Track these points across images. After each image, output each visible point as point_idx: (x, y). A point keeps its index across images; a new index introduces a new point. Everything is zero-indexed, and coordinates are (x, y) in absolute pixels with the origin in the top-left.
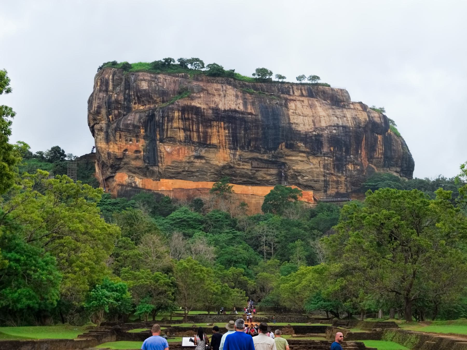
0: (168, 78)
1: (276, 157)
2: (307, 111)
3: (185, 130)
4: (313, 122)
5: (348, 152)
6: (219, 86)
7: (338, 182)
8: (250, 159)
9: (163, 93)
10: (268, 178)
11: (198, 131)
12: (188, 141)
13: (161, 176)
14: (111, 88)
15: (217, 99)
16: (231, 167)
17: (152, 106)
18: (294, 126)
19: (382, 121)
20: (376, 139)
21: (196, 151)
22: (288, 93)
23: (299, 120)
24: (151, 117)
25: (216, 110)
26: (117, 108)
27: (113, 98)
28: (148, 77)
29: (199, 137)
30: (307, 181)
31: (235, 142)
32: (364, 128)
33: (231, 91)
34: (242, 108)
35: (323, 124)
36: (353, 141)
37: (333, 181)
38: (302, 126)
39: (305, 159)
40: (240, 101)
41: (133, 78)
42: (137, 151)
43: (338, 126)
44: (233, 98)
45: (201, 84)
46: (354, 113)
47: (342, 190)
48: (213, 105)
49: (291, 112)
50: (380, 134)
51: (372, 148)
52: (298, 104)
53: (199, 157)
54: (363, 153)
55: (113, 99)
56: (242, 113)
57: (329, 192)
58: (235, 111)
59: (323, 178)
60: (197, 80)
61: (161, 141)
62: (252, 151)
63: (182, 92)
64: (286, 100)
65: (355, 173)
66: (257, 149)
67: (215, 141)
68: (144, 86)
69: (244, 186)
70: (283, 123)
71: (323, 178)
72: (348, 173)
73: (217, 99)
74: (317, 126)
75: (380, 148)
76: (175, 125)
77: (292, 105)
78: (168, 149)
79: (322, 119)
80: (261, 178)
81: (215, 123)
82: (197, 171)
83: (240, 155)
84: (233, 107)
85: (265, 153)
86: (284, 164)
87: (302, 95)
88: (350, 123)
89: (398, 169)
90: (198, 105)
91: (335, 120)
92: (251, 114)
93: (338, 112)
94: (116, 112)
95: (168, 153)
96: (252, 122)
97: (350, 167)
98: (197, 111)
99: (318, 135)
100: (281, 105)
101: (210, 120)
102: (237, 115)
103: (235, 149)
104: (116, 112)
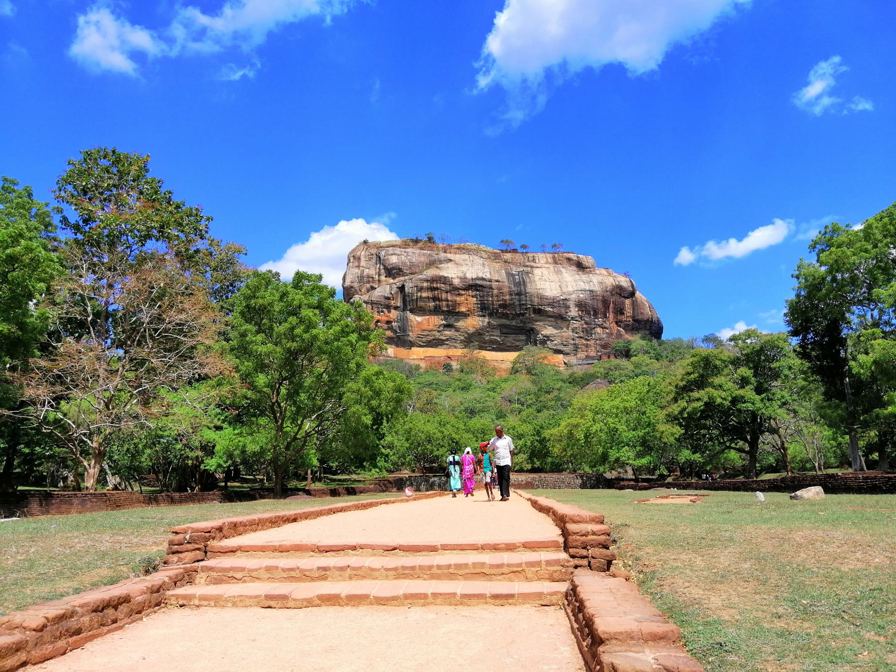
0: (418, 251)
1: (525, 323)
2: (554, 277)
3: (435, 299)
4: (560, 287)
5: (596, 314)
6: (466, 257)
7: (587, 346)
8: (499, 325)
9: (412, 265)
10: (517, 343)
11: (447, 300)
12: (436, 311)
13: (411, 345)
14: (363, 263)
15: (464, 268)
16: (480, 334)
17: (402, 278)
18: (541, 291)
19: (630, 284)
20: (624, 304)
21: (445, 319)
22: (534, 260)
23: (547, 285)
24: (402, 289)
25: (463, 279)
26: (368, 282)
27: (365, 273)
28: (398, 251)
29: (448, 306)
30: (556, 345)
31: (484, 308)
32: (611, 292)
33: (478, 260)
34: (488, 276)
35: (570, 289)
36: (600, 305)
37: (584, 345)
38: (549, 290)
39: (554, 324)
40: (487, 270)
41: (383, 253)
42: (388, 322)
43: (585, 291)
44: (481, 267)
45: (449, 256)
46: (600, 278)
47: (592, 354)
48: (461, 275)
49: (537, 278)
50: (628, 298)
51: (620, 311)
52: (545, 271)
53: (448, 326)
54: (611, 316)
55: (365, 273)
56: (490, 281)
57: (578, 356)
58: (483, 279)
59: (572, 342)
60: (445, 252)
61: (412, 311)
62: (500, 318)
63: (432, 264)
64: (532, 267)
65: (604, 336)
66: (505, 316)
67: (463, 309)
68: (394, 260)
69: (494, 353)
70: (530, 289)
71: (572, 342)
72: (598, 336)
73: (464, 268)
74: (565, 290)
75: (628, 311)
76: (424, 295)
77: (537, 272)
78: (419, 319)
79: (569, 284)
80: (509, 344)
81: (463, 292)
82: (447, 340)
83: (489, 323)
84: (480, 275)
85: (513, 319)
86: (532, 330)
87: (547, 263)
88: (597, 288)
89: (647, 332)
90: (446, 275)
91: (583, 286)
92: (497, 281)
93: (584, 277)
94: (368, 286)
95: (419, 323)
96: (499, 289)
97: (599, 330)
98: (445, 280)
99: (566, 299)
100: (528, 273)
101: (457, 289)
102: (484, 283)
103: (484, 316)
104: (368, 286)
